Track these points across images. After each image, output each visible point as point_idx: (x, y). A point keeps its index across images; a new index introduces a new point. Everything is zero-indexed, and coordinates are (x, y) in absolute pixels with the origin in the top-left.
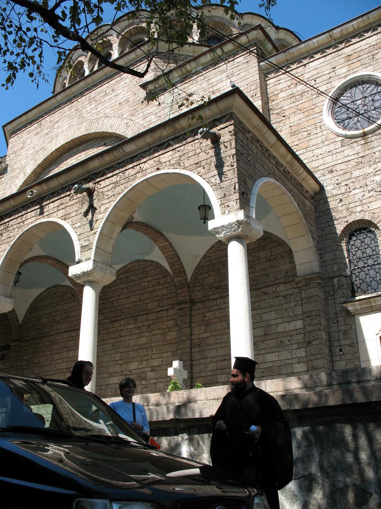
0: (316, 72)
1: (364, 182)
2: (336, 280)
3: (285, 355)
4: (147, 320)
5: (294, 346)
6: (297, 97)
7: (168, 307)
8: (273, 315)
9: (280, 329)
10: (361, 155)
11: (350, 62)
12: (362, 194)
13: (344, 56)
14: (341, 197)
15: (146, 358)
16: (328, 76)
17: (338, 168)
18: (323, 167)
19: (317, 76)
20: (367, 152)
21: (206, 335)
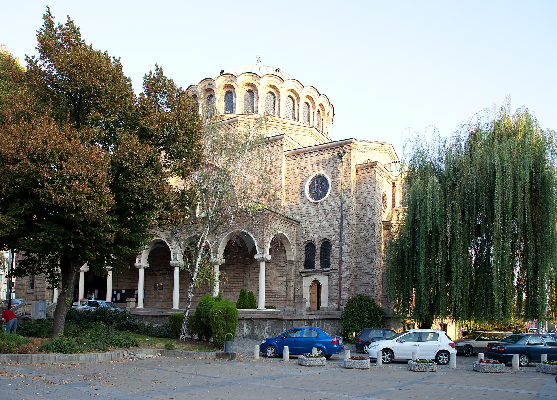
0: (305, 164)
2: (299, 263)
3: (280, 289)
4: (233, 267)
5: (283, 286)
6: (297, 175)
7: (241, 263)
8: (277, 273)
9: (279, 279)
10: (315, 212)
12: (312, 229)
13: (316, 160)
14: (305, 229)
15: (232, 283)
16: (309, 169)
17: (307, 215)
18: (301, 213)
20: (317, 211)
21: (255, 277)
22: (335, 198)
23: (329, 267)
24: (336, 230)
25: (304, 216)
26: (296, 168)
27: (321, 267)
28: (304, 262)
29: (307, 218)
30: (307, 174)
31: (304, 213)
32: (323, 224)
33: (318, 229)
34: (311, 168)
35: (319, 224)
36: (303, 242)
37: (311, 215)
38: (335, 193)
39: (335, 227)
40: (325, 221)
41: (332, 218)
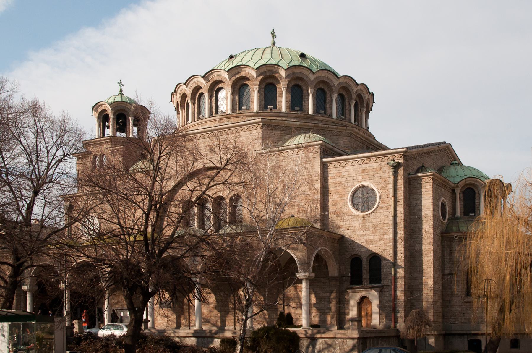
1: (360, 238)
11: (363, 174)
13: (361, 169)
14: (350, 242)
16: (352, 178)
17: (351, 228)
18: (345, 226)
19: (348, 176)
20: (364, 224)
22: (385, 211)
23: (380, 283)
24: (388, 244)
25: (348, 229)
26: (336, 177)
27: (370, 283)
28: (350, 278)
29: (352, 231)
30: (350, 184)
31: (348, 226)
32: (371, 238)
33: (366, 243)
34: (355, 178)
35: (366, 238)
36: (347, 256)
37: (357, 228)
38: (385, 205)
39: (386, 241)
40: (373, 234)
41: (382, 231)
